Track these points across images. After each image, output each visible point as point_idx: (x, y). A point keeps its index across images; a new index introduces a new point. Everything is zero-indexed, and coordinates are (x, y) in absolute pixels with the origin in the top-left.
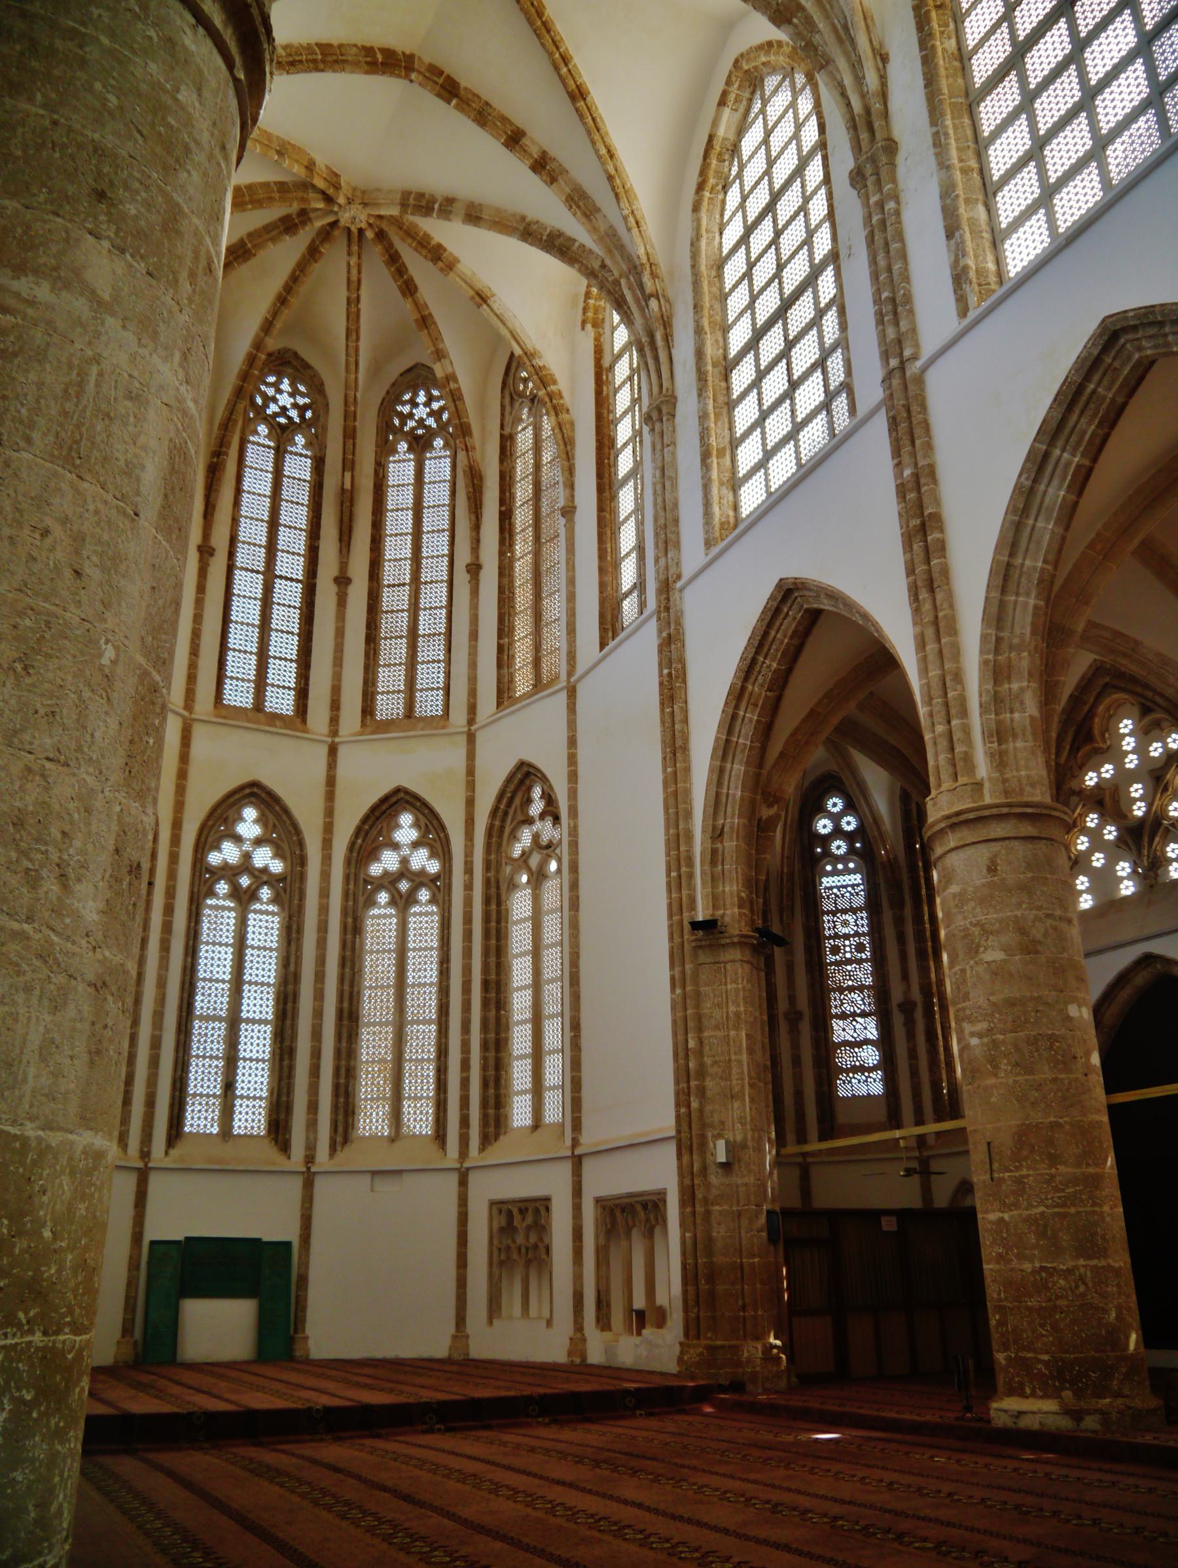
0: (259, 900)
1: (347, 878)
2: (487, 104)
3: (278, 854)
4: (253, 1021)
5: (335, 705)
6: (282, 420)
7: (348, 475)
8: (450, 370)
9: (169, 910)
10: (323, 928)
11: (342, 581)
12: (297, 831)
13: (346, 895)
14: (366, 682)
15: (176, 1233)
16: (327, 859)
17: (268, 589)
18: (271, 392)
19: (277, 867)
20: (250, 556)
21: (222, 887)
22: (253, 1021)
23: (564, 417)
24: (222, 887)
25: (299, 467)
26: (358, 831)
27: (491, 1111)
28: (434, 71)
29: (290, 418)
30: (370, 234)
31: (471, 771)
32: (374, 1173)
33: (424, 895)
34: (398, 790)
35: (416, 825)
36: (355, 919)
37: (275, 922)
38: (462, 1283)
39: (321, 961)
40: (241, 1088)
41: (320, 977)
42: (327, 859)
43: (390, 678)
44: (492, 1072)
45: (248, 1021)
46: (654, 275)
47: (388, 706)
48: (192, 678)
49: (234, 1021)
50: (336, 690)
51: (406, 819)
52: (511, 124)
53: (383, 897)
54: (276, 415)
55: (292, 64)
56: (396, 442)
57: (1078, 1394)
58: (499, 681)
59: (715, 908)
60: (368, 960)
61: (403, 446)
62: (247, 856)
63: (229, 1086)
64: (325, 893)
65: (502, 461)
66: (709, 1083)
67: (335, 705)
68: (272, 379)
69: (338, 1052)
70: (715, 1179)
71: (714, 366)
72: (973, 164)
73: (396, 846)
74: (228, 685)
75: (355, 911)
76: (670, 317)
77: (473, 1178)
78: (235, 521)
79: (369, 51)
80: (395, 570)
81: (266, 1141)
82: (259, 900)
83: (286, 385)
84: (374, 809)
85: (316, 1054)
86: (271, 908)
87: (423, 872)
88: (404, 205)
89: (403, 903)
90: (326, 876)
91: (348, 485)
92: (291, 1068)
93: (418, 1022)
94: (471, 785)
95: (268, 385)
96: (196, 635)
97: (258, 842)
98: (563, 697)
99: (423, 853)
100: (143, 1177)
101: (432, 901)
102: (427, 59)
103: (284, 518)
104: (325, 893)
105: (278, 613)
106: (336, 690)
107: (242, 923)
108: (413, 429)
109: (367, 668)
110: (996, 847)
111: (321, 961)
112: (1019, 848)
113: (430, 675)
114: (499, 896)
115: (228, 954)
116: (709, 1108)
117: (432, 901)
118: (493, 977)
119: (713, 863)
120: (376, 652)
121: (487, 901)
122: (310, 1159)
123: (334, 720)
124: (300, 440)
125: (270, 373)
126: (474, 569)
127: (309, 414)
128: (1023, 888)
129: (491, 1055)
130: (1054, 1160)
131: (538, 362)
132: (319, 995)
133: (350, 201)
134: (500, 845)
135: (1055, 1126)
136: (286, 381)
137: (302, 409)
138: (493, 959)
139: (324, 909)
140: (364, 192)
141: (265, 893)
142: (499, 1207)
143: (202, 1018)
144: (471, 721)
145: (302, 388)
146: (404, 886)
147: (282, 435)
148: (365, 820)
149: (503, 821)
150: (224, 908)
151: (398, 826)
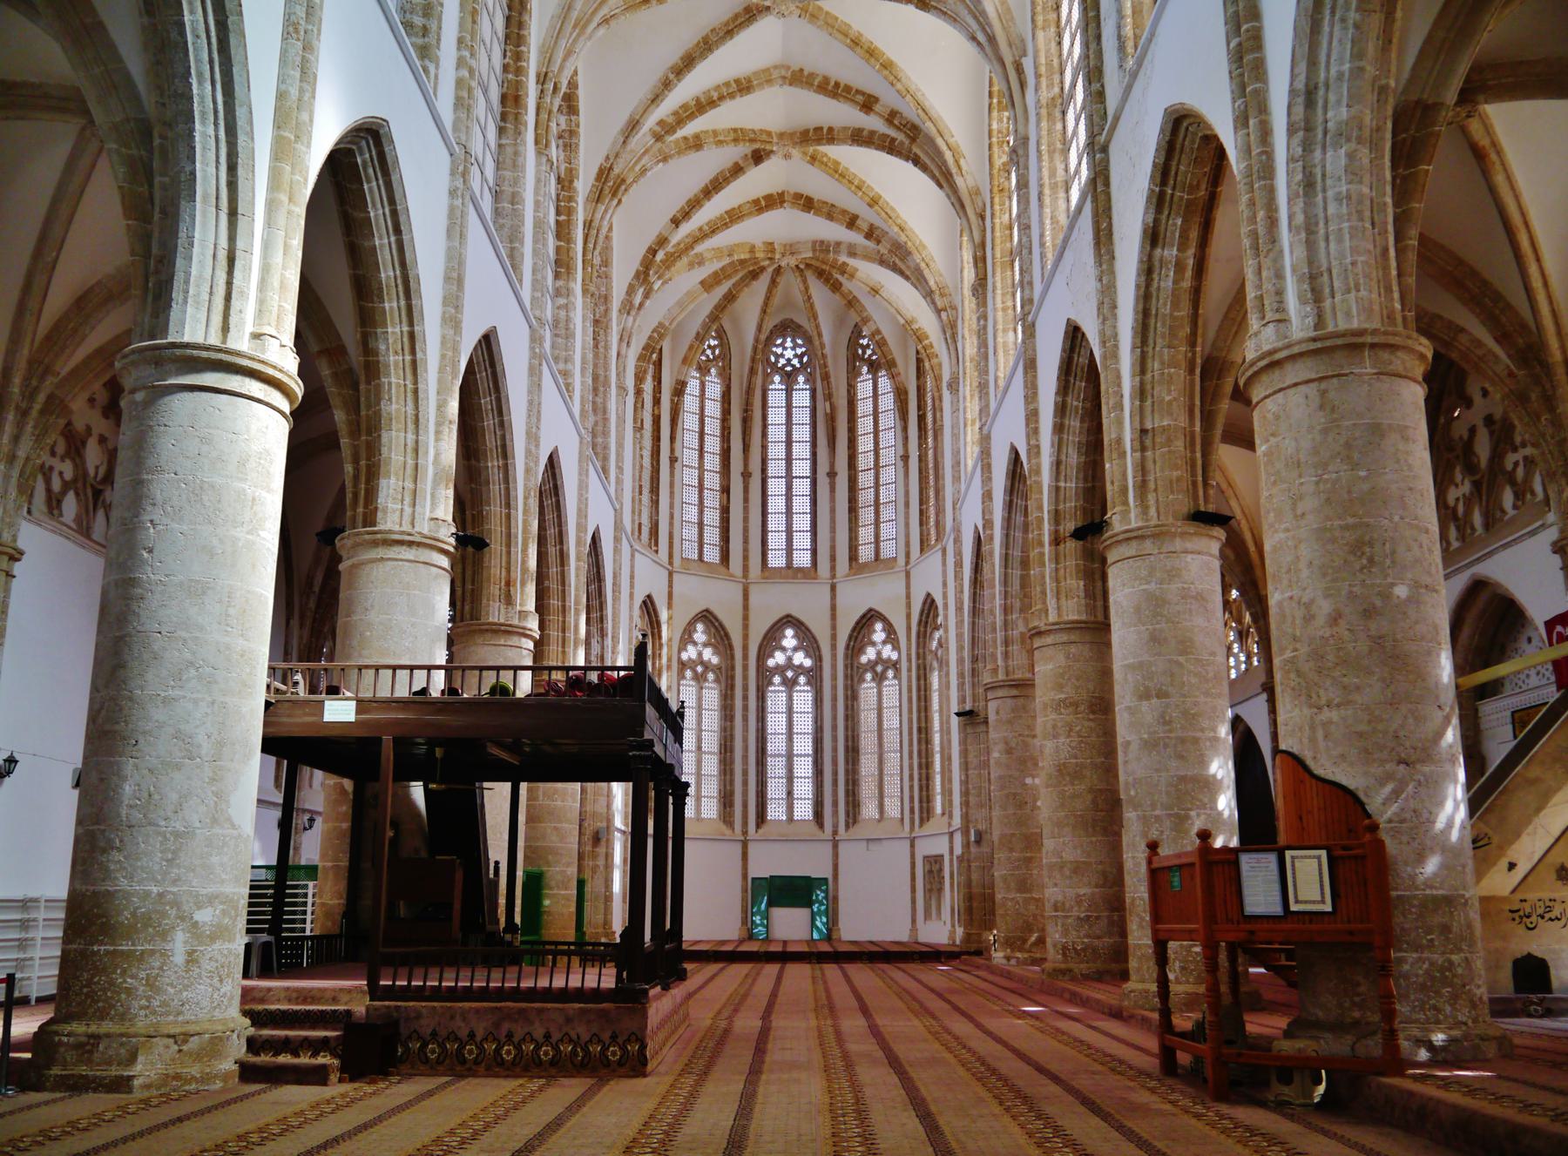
0: (799, 684)
1: (846, 666)
2: (833, 205)
3: (807, 655)
4: (801, 756)
5: (833, 559)
6: (789, 369)
7: (828, 404)
8: (874, 328)
9: (745, 698)
10: (834, 699)
11: (832, 474)
12: (816, 641)
13: (846, 676)
14: (851, 539)
15: (765, 874)
16: (834, 656)
17: (789, 488)
18: (779, 351)
19: (808, 663)
20: (776, 468)
21: (777, 679)
22: (801, 756)
23: (935, 361)
24: (777, 679)
25: (802, 398)
26: (850, 637)
27: (925, 805)
28: (798, 196)
29: (793, 366)
30: (802, 266)
31: (908, 596)
32: (868, 840)
33: (890, 673)
34: (870, 610)
35: (884, 630)
36: (853, 691)
37: (809, 697)
38: (914, 901)
39: (834, 718)
40: (797, 793)
41: (834, 728)
42: (834, 656)
43: (866, 534)
44: (924, 782)
45: (798, 755)
46: (942, 295)
47: (865, 553)
48: (746, 558)
49: (790, 756)
50: (833, 548)
51: (879, 626)
52: (848, 213)
53: (869, 676)
54: (784, 366)
55: (713, 232)
56: (861, 367)
57: (1013, 951)
58: (921, 535)
59: (974, 701)
60: (862, 716)
61: (865, 369)
62: (790, 659)
63: (790, 793)
64: (834, 677)
65: (918, 378)
66: (971, 799)
67: (833, 559)
68: (779, 342)
69: (847, 771)
70: (973, 849)
71: (971, 361)
72: (1010, 304)
73: (873, 644)
74: (770, 554)
75: (852, 686)
76: (955, 321)
77: (917, 842)
78: (764, 447)
79: (756, 202)
80: (865, 461)
81: (813, 823)
82: (799, 684)
83: (789, 344)
84: (857, 623)
85: (835, 773)
86: (806, 688)
87: (889, 659)
88: (814, 250)
89: (880, 679)
90: (834, 667)
91: (828, 411)
92: (822, 781)
93: (890, 752)
94: (909, 605)
95: (777, 346)
96: (746, 530)
97: (795, 649)
98: (940, 553)
99: (889, 647)
100: (745, 844)
101: (895, 677)
102: (792, 192)
103: (795, 437)
104: (834, 677)
105: (796, 502)
106: (833, 548)
107: (790, 699)
108: (870, 356)
109: (850, 530)
110: (999, 701)
111: (834, 718)
112: (1009, 701)
113: (887, 530)
114: (925, 675)
115: (783, 719)
116: (971, 812)
117: (895, 677)
118: (923, 725)
119: (973, 675)
120: (856, 518)
121: (918, 679)
122: (835, 832)
123: (833, 568)
124: (801, 379)
125: (778, 337)
126: (905, 458)
127: (805, 359)
128: (1010, 722)
129: (924, 771)
130: (1011, 850)
131: (915, 326)
132: (835, 739)
133: (783, 255)
134: (925, 643)
135: (1013, 835)
136: (789, 340)
137: (800, 357)
138: (923, 714)
139: (834, 688)
140: (791, 245)
141: (802, 679)
142: (927, 859)
143: (771, 756)
144: (907, 563)
145: (799, 342)
146: (879, 668)
147: (789, 378)
148: (854, 630)
149: (926, 627)
150: (779, 691)
151: (875, 631)
